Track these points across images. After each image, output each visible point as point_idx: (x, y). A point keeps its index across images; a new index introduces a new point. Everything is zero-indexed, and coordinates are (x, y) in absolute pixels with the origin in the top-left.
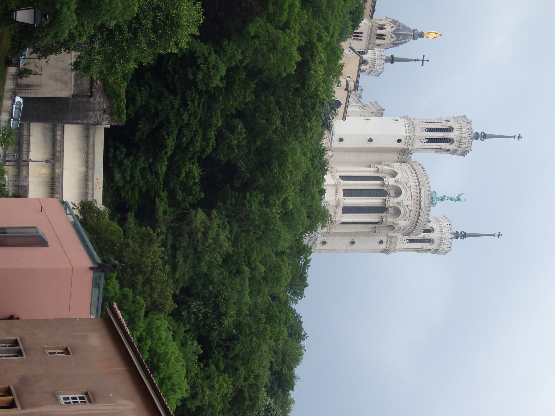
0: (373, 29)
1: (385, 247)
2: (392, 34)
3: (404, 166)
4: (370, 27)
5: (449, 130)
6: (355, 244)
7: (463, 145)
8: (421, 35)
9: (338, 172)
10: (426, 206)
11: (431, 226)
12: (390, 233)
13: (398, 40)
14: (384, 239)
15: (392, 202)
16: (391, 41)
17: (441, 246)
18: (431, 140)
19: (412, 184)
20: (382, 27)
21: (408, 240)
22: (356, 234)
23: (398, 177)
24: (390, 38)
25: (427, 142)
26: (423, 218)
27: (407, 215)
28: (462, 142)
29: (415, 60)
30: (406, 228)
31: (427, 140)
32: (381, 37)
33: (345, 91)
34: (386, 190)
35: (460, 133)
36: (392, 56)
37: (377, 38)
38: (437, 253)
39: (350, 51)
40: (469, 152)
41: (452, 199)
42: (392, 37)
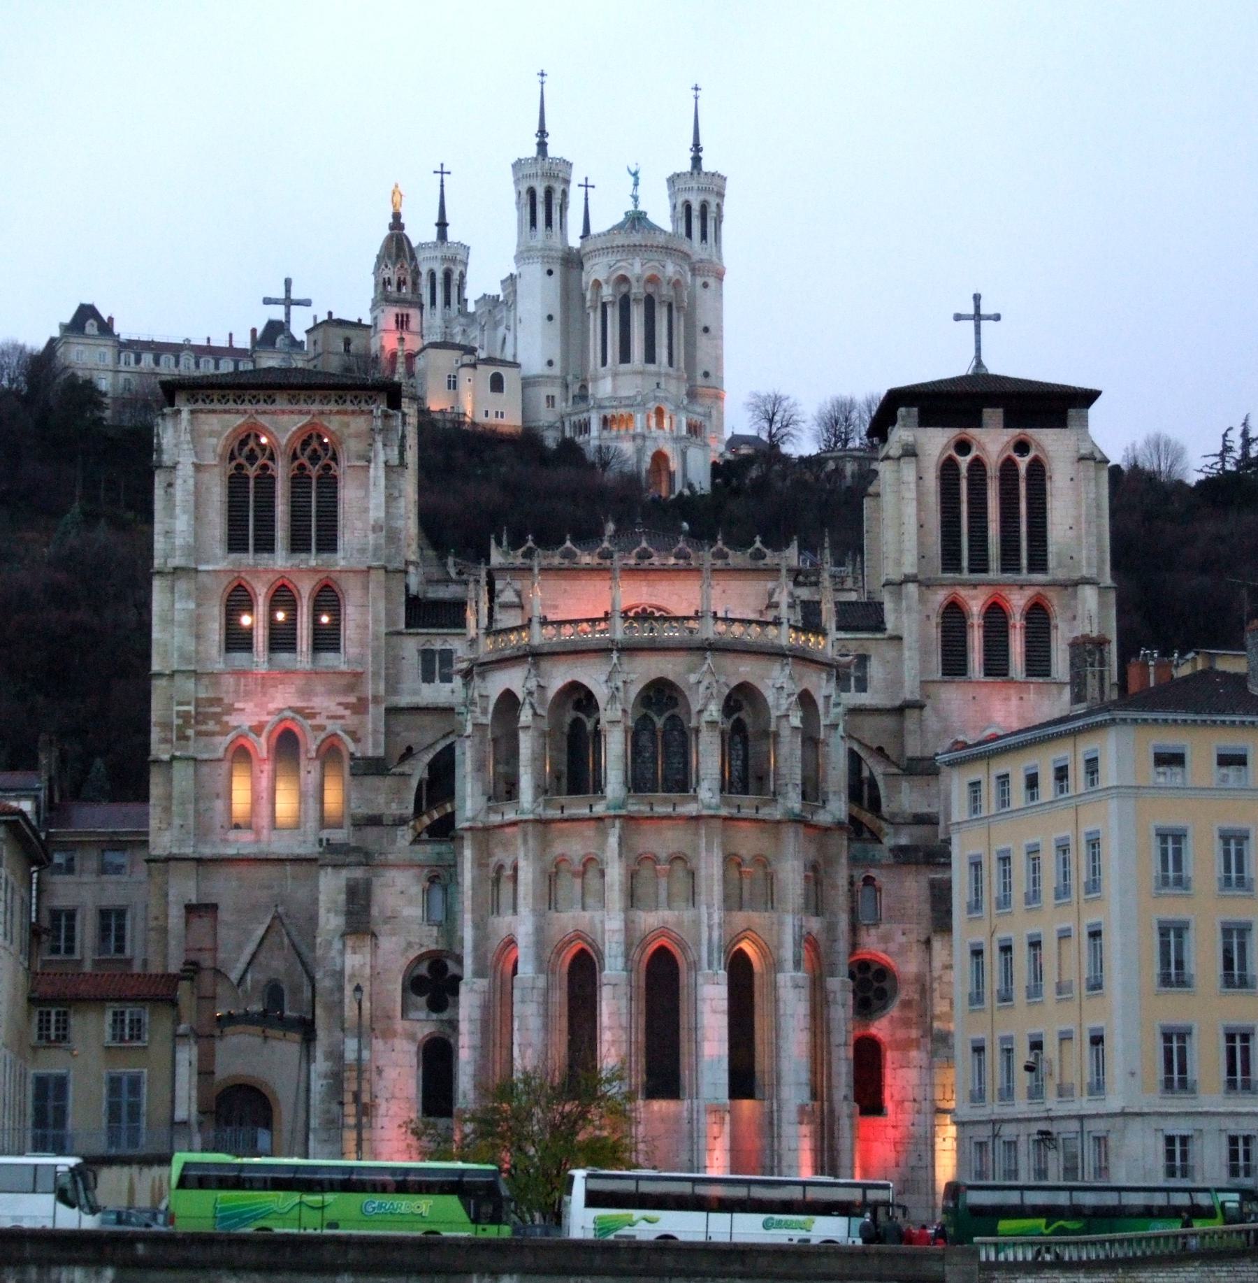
3: (587, 266)
5: (532, 192)
8: (397, 216)
14: (699, 281)
15: (637, 290)
18: (549, 222)
20: (387, 282)
23: (601, 279)
27: (656, 264)
29: (442, 186)
36: (437, 225)
41: (636, 184)
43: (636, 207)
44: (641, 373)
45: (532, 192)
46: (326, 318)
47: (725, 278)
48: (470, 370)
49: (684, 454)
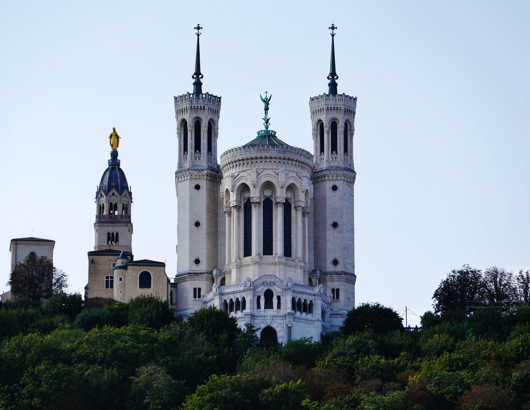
0: (103, 220)
1: (340, 180)
2: (109, 195)
4: (100, 225)
6: (337, 220)
8: (114, 154)
10: (258, 151)
14: (329, 185)
16: (118, 195)
17: (339, 108)
21: (332, 152)
24: (114, 197)
25: (200, 151)
26: (273, 152)
27: (271, 172)
28: (198, 107)
31: (198, 151)
34: (245, 201)
35: (187, 110)
41: (267, 109)
43: (267, 127)
48: (123, 270)
49: (290, 329)
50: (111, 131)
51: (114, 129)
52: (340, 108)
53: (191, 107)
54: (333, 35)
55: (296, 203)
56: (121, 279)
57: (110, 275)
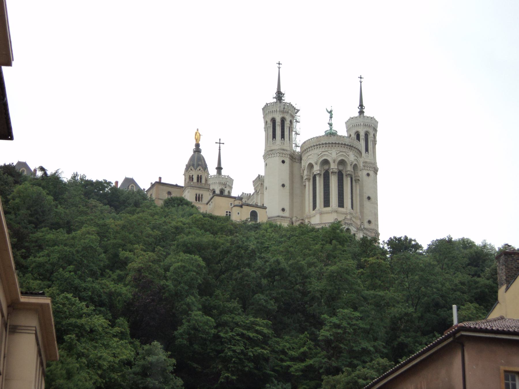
0: (193, 185)
1: (372, 171)
3: (304, 158)
5: (274, 121)
6: (370, 196)
7: (286, 109)
8: (197, 145)
9: (310, 212)
11: (354, 133)
12: (360, 168)
13: (201, 165)
14: (365, 172)
15: (334, 167)
18: (283, 136)
19: (318, 151)
20: (191, 178)
22: (361, 195)
23: (313, 162)
24: (200, 172)
25: (284, 139)
27: (344, 154)
28: (284, 111)
29: (220, 150)
30: (355, 154)
32: (199, 178)
33: (242, 208)
34: (324, 172)
36: (217, 168)
37: (201, 182)
38: (376, 128)
39: (210, 204)
40: (291, 105)
41: (331, 117)
42: (200, 170)
43: (331, 129)
44: (336, 212)
45: (274, 121)
46: (158, 180)
47: (378, 173)
48: (239, 208)
50: (196, 131)
51: (198, 130)
52: (371, 125)
53: (280, 110)
54: (361, 82)
55: (356, 177)
56: (238, 213)
57: (228, 211)
